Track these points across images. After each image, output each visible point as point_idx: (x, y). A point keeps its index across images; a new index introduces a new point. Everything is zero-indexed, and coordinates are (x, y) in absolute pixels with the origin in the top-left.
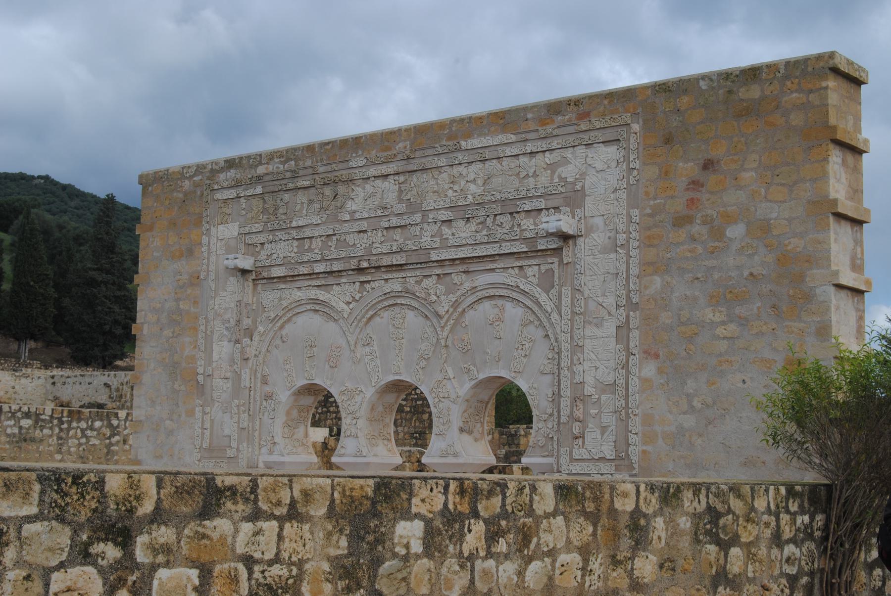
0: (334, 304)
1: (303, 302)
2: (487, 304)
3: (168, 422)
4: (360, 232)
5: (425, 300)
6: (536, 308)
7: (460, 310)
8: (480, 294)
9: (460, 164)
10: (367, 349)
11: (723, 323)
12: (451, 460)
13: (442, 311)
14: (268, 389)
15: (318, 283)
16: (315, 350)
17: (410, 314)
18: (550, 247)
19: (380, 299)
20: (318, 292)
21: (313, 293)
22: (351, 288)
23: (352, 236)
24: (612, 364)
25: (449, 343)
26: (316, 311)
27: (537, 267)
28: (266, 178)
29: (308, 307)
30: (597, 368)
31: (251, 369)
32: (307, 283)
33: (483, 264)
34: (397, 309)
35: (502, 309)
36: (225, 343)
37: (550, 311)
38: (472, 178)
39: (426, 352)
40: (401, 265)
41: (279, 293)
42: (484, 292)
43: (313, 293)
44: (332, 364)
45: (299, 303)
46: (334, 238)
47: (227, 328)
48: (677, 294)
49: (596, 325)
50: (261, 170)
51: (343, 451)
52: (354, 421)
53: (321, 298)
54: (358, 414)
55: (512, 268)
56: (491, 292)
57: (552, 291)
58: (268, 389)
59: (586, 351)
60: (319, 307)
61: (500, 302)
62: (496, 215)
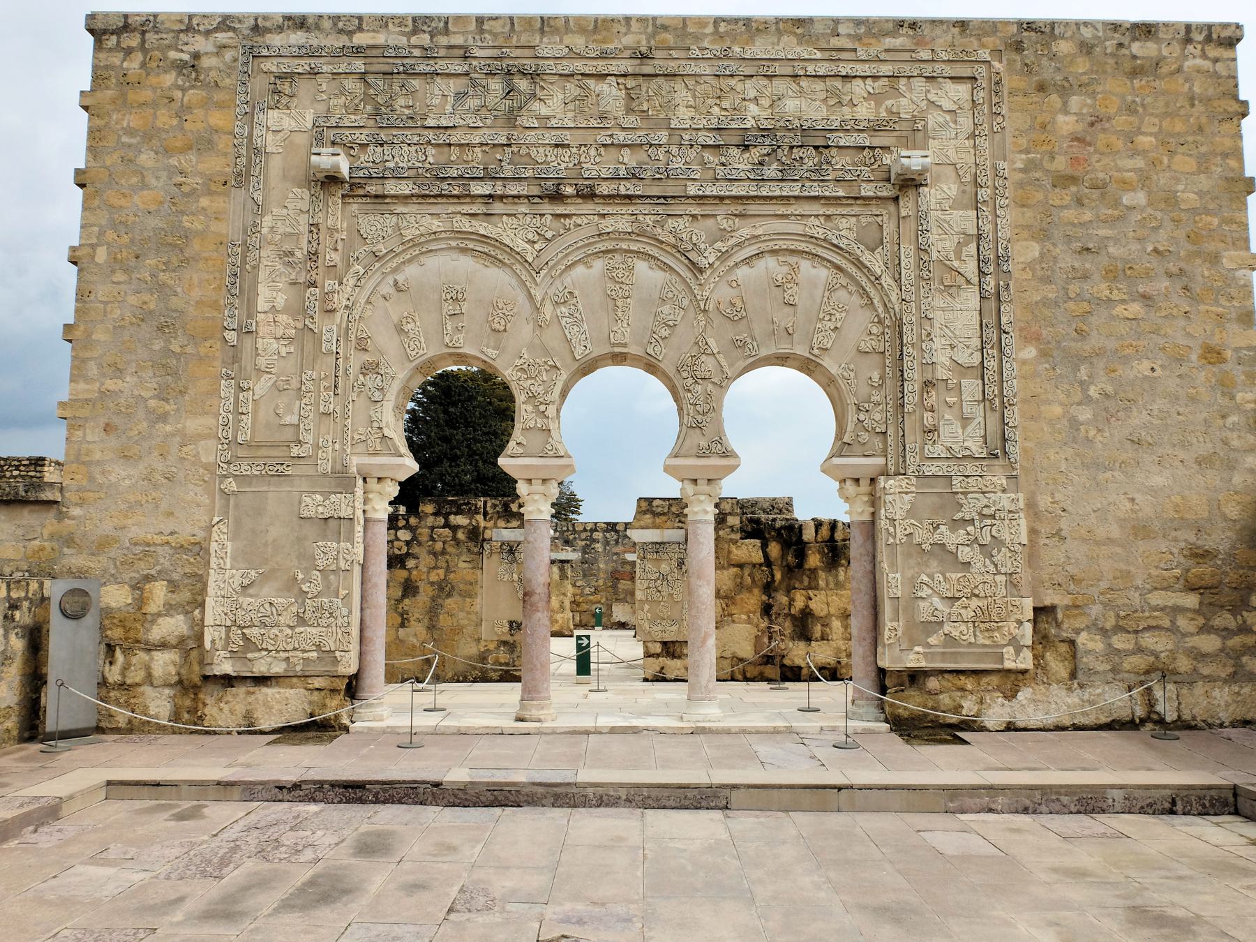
0: (507, 242)
2: (770, 262)
3: (153, 403)
4: (557, 146)
5: (674, 247)
8: (763, 247)
9: (732, 76)
11: (1123, 301)
13: (703, 263)
15: (475, 209)
16: (465, 306)
17: (641, 266)
18: (880, 194)
19: (591, 240)
20: (474, 222)
21: (465, 225)
22: (537, 221)
23: (541, 150)
24: (976, 342)
25: (711, 307)
26: (464, 250)
27: (854, 219)
28: (369, 52)
29: (454, 244)
31: (339, 326)
32: (451, 209)
33: (771, 207)
34: (618, 257)
35: (795, 269)
38: (752, 96)
39: (671, 317)
41: (395, 219)
42: (771, 244)
43: (465, 225)
44: (497, 327)
49: (951, 295)
50: (360, 39)
52: (542, 408)
53: (482, 232)
54: (549, 398)
55: (816, 216)
57: (880, 249)
58: (367, 357)
59: (937, 325)
60: (469, 244)
61: (793, 259)
62: (792, 147)
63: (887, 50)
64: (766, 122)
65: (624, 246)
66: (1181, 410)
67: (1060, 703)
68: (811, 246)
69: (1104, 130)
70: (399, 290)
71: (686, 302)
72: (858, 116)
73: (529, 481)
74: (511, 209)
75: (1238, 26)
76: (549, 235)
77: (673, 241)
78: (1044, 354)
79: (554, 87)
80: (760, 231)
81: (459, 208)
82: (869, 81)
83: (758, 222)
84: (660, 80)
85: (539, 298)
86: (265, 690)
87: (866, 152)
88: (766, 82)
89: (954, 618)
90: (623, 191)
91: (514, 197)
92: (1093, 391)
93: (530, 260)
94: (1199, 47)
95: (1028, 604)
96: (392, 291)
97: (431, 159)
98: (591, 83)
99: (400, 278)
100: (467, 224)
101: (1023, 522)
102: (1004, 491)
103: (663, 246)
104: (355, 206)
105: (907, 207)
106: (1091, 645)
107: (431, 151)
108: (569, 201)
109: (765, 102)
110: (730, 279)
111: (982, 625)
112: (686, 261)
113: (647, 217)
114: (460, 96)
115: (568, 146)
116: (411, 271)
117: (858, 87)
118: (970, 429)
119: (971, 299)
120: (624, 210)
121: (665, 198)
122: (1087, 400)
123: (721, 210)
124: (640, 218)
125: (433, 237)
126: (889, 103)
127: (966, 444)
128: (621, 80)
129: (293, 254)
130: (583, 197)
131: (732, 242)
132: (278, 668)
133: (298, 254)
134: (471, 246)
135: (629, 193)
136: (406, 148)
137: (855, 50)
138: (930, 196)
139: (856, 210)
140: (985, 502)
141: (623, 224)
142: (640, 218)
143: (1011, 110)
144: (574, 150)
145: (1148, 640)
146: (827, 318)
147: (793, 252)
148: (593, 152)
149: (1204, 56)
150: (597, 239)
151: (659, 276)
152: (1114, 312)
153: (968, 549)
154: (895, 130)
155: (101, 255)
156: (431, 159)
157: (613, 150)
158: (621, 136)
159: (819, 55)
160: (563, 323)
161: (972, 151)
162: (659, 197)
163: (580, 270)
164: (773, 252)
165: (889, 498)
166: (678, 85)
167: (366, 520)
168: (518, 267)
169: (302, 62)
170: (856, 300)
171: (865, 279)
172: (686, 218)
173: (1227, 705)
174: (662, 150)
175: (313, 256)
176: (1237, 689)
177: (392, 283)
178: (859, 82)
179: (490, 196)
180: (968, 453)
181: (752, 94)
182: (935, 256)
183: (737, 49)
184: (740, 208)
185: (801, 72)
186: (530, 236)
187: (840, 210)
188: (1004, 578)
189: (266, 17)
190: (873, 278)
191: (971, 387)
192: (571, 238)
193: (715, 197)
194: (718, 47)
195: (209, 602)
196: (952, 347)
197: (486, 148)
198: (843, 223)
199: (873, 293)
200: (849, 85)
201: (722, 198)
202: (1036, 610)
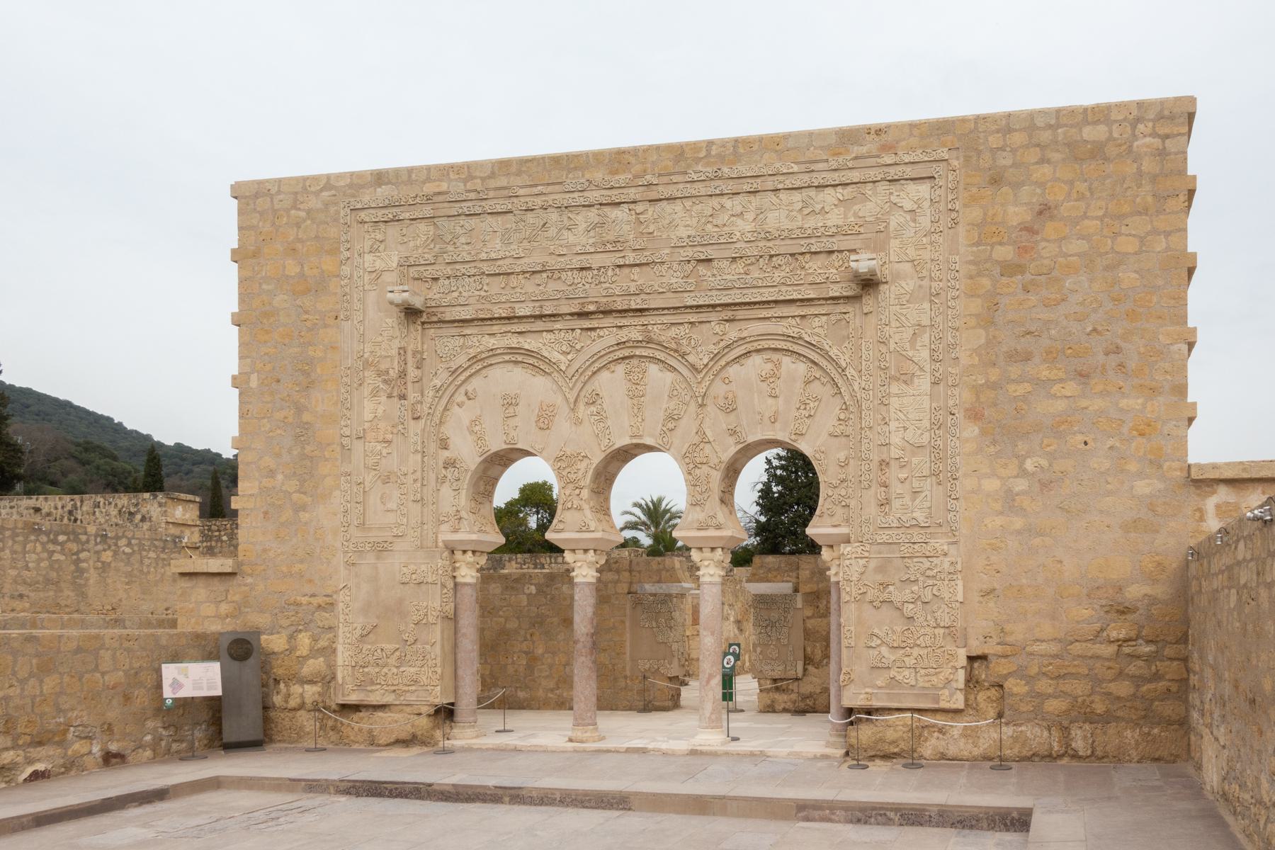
0: (546, 354)
2: (757, 359)
3: (295, 496)
4: (582, 269)
5: (676, 351)
6: (823, 363)
7: (723, 363)
8: (750, 347)
10: (593, 409)
11: (1061, 380)
12: (712, 533)
13: (700, 365)
14: (446, 454)
15: (521, 328)
17: (653, 369)
20: (521, 339)
21: (514, 341)
22: (570, 336)
24: (926, 423)
26: (516, 362)
27: (825, 318)
28: (436, 199)
29: (507, 358)
30: (905, 429)
32: (504, 329)
34: (635, 362)
35: (778, 365)
36: (384, 399)
37: (844, 365)
40: (641, 310)
42: (755, 344)
46: (544, 275)
47: (385, 381)
48: (1005, 349)
49: (905, 382)
51: (561, 526)
53: (527, 347)
54: (582, 483)
56: (765, 344)
59: (892, 410)
61: (775, 356)
62: (771, 256)
63: (856, 158)
64: (749, 235)
65: (638, 352)
66: (1110, 479)
67: (989, 735)
68: (789, 344)
69: (1052, 218)
71: (688, 398)
72: (829, 223)
73: (573, 551)
74: (549, 325)
75: (1192, 100)
76: (578, 347)
77: (674, 346)
78: (984, 432)
79: (579, 217)
80: (745, 334)
81: (508, 328)
82: (839, 189)
83: (743, 325)
84: (664, 203)
85: (572, 400)
86: (380, 714)
87: (834, 256)
88: (752, 198)
89: (898, 664)
90: (634, 306)
92: (1029, 465)
94: (1150, 124)
95: (962, 654)
96: (463, 398)
97: (485, 288)
98: (607, 209)
101: (960, 583)
102: (946, 555)
105: (868, 303)
106: (1015, 690)
107: (486, 280)
109: (750, 216)
111: (923, 672)
115: (589, 268)
116: (476, 383)
117: (829, 196)
118: (917, 501)
119: (924, 384)
122: (1023, 473)
123: (713, 316)
124: (650, 327)
126: (856, 207)
127: (915, 515)
128: (632, 206)
130: (602, 312)
131: (722, 344)
132: (389, 699)
133: (391, 372)
136: (467, 280)
137: (827, 161)
138: (888, 293)
140: (927, 564)
141: (636, 335)
144: (595, 272)
145: (1067, 686)
147: (776, 350)
149: (1154, 134)
151: (669, 376)
152: (1052, 391)
153: (911, 606)
154: (860, 233)
155: (254, 382)
157: (626, 270)
158: (631, 258)
159: (796, 168)
162: (664, 309)
163: (605, 375)
164: (758, 351)
165: (847, 562)
166: (678, 206)
167: (456, 585)
169: (386, 211)
170: (829, 390)
171: (834, 371)
173: (1137, 743)
174: (665, 266)
175: (403, 374)
176: (1146, 730)
178: (830, 190)
180: (914, 522)
181: (739, 209)
183: (726, 170)
185: (780, 186)
186: (564, 348)
188: (942, 631)
189: (360, 175)
191: (921, 462)
193: (708, 306)
194: (709, 169)
195: (340, 648)
198: (816, 322)
199: (840, 383)
200: (821, 195)
201: (714, 306)
202: (971, 659)
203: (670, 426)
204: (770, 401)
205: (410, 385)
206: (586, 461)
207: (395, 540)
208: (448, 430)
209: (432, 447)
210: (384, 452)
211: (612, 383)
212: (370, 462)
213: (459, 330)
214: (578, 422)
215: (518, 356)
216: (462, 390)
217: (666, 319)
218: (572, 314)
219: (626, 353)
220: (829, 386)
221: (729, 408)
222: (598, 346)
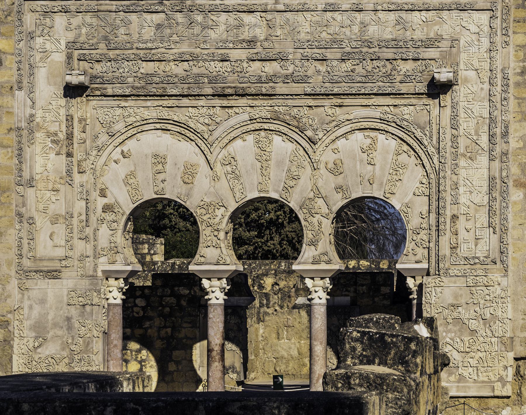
1: (151, 121)
2: (359, 135)
4: (222, 61)
7: (333, 137)
10: (229, 168)
17: (277, 139)
19: (245, 123)
21: (165, 114)
23: (212, 63)
24: (485, 189)
29: (158, 126)
30: (471, 192)
32: (156, 103)
34: (263, 133)
35: (374, 141)
36: (52, 156)
45: (145, 122)
46: (191, 63)
47: (53, 142)
49: (470, 158)
61: (373, 134)
65: (266, 126)
70: (124, 157)
74: (194, 103)
77: (296, 123)
81: (160, 103)
84: (289, 15)
90: (264, 91)
91: (195, 96)
93: (206, 137)
99: (125, 148)
100: (166, 114)
103: (290, 127)
104: (95, 102)
108: (231, 98)
110: (333, 147)
112: (305, 137)
113: (281, 108)
114: (159, 26)
116: (130, 145)
119: (484, 160)
120: (265, 103)
121: (291, 95)
123: (327, 102)
125: (145, 122)
129: (56, 135)
130: (239, 95)
134: (169, 127)
135: (268, 93)
138: (461, 92)
139: (414, 101)
141: (265, 113)
142: (276, 108)
143: (514, 33)
146: (394, 173)
148: (245, 65)
150: (249, 122)
156: (142, 71)
160: (228, 178)
161: (489, 60)
162: (287, 95)
163: (238, 142)
168: (199, 142)
170: (413, 160)
172: (305, 108)
177: (120, 151)
179: (180, 95)
182: (461, 131)
184: (339, 101)
186: (206, 121)
187: (403, 102)
190: (422, 147)
192: (232, 121)
196: (471, 192)
197: (177, 62)
203: (292, 183)
204: (370, 167)
205: (76, 145)
206: (223, 209)
207: (63, 269)
208: (107, 179)
209: (95, 195)
210: (53, 198)
211: (244, 148)
212: (41, 207)
213: (118, 102)
214: (216, 178)
215: (164, 125)
216: (119, 149)
217: (290, 102)
218: (213, 95)
219: (257, 126)
220: (413, 157)
221: (336, 170)
222: (232, 121)
